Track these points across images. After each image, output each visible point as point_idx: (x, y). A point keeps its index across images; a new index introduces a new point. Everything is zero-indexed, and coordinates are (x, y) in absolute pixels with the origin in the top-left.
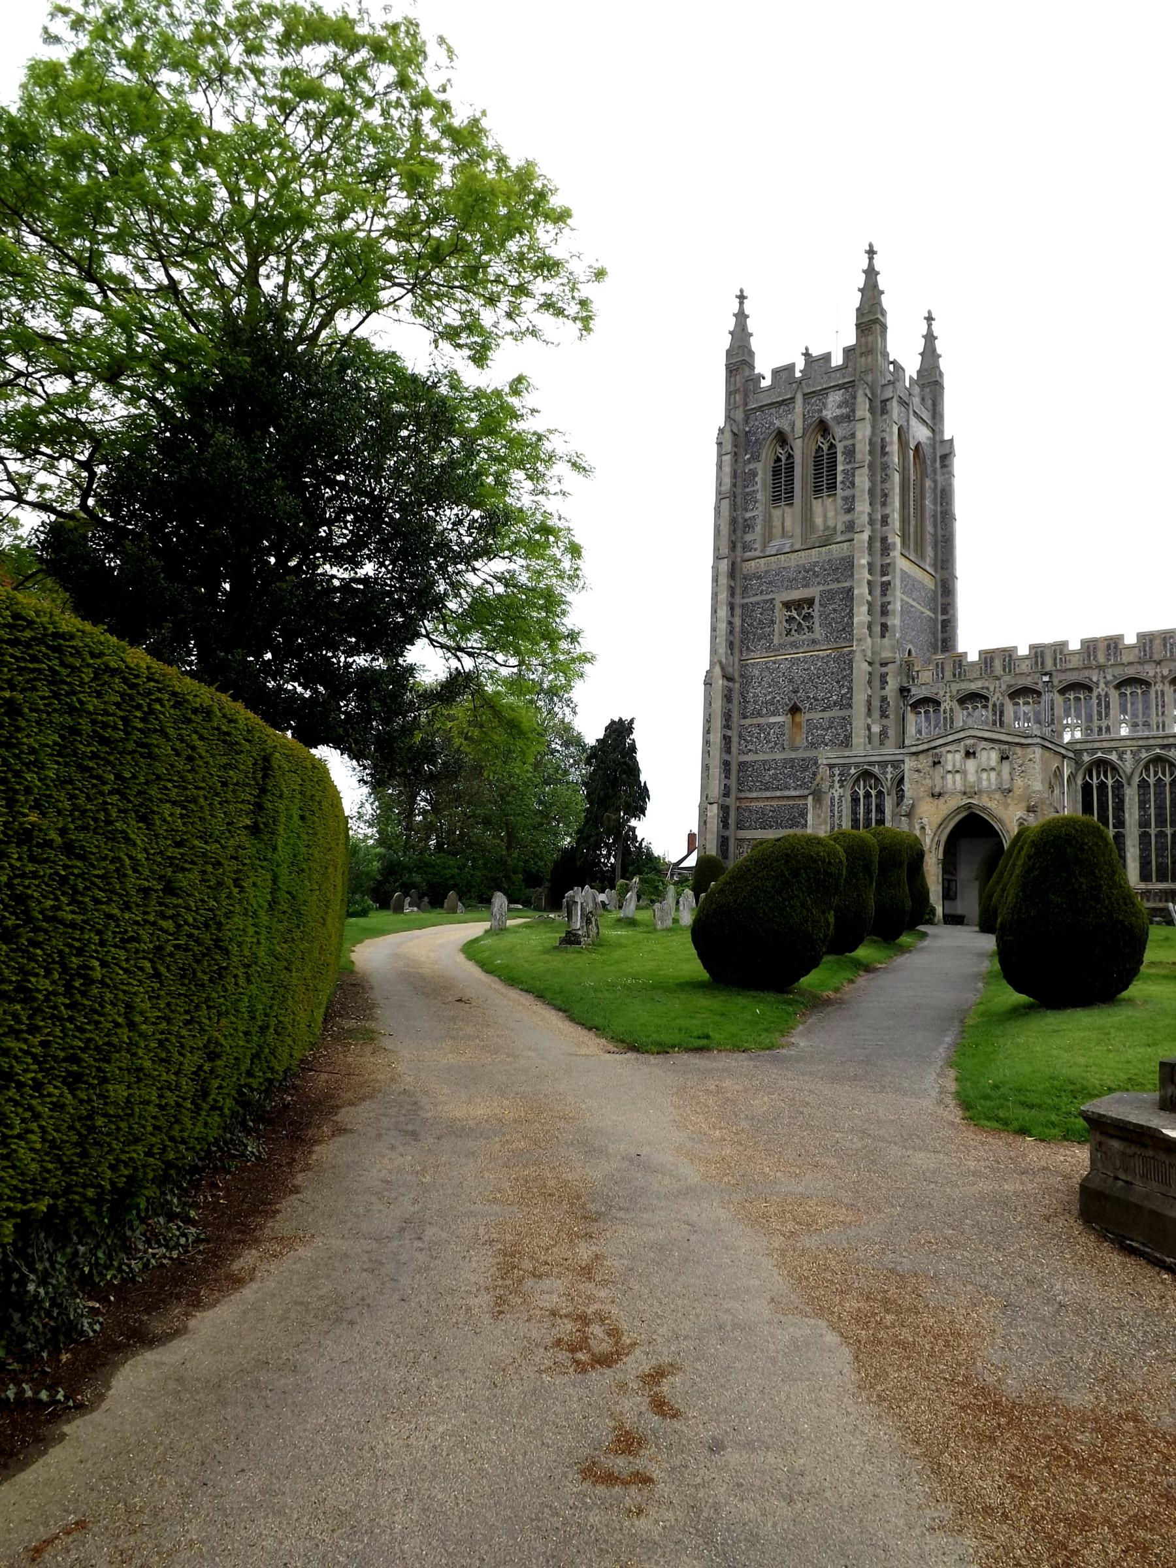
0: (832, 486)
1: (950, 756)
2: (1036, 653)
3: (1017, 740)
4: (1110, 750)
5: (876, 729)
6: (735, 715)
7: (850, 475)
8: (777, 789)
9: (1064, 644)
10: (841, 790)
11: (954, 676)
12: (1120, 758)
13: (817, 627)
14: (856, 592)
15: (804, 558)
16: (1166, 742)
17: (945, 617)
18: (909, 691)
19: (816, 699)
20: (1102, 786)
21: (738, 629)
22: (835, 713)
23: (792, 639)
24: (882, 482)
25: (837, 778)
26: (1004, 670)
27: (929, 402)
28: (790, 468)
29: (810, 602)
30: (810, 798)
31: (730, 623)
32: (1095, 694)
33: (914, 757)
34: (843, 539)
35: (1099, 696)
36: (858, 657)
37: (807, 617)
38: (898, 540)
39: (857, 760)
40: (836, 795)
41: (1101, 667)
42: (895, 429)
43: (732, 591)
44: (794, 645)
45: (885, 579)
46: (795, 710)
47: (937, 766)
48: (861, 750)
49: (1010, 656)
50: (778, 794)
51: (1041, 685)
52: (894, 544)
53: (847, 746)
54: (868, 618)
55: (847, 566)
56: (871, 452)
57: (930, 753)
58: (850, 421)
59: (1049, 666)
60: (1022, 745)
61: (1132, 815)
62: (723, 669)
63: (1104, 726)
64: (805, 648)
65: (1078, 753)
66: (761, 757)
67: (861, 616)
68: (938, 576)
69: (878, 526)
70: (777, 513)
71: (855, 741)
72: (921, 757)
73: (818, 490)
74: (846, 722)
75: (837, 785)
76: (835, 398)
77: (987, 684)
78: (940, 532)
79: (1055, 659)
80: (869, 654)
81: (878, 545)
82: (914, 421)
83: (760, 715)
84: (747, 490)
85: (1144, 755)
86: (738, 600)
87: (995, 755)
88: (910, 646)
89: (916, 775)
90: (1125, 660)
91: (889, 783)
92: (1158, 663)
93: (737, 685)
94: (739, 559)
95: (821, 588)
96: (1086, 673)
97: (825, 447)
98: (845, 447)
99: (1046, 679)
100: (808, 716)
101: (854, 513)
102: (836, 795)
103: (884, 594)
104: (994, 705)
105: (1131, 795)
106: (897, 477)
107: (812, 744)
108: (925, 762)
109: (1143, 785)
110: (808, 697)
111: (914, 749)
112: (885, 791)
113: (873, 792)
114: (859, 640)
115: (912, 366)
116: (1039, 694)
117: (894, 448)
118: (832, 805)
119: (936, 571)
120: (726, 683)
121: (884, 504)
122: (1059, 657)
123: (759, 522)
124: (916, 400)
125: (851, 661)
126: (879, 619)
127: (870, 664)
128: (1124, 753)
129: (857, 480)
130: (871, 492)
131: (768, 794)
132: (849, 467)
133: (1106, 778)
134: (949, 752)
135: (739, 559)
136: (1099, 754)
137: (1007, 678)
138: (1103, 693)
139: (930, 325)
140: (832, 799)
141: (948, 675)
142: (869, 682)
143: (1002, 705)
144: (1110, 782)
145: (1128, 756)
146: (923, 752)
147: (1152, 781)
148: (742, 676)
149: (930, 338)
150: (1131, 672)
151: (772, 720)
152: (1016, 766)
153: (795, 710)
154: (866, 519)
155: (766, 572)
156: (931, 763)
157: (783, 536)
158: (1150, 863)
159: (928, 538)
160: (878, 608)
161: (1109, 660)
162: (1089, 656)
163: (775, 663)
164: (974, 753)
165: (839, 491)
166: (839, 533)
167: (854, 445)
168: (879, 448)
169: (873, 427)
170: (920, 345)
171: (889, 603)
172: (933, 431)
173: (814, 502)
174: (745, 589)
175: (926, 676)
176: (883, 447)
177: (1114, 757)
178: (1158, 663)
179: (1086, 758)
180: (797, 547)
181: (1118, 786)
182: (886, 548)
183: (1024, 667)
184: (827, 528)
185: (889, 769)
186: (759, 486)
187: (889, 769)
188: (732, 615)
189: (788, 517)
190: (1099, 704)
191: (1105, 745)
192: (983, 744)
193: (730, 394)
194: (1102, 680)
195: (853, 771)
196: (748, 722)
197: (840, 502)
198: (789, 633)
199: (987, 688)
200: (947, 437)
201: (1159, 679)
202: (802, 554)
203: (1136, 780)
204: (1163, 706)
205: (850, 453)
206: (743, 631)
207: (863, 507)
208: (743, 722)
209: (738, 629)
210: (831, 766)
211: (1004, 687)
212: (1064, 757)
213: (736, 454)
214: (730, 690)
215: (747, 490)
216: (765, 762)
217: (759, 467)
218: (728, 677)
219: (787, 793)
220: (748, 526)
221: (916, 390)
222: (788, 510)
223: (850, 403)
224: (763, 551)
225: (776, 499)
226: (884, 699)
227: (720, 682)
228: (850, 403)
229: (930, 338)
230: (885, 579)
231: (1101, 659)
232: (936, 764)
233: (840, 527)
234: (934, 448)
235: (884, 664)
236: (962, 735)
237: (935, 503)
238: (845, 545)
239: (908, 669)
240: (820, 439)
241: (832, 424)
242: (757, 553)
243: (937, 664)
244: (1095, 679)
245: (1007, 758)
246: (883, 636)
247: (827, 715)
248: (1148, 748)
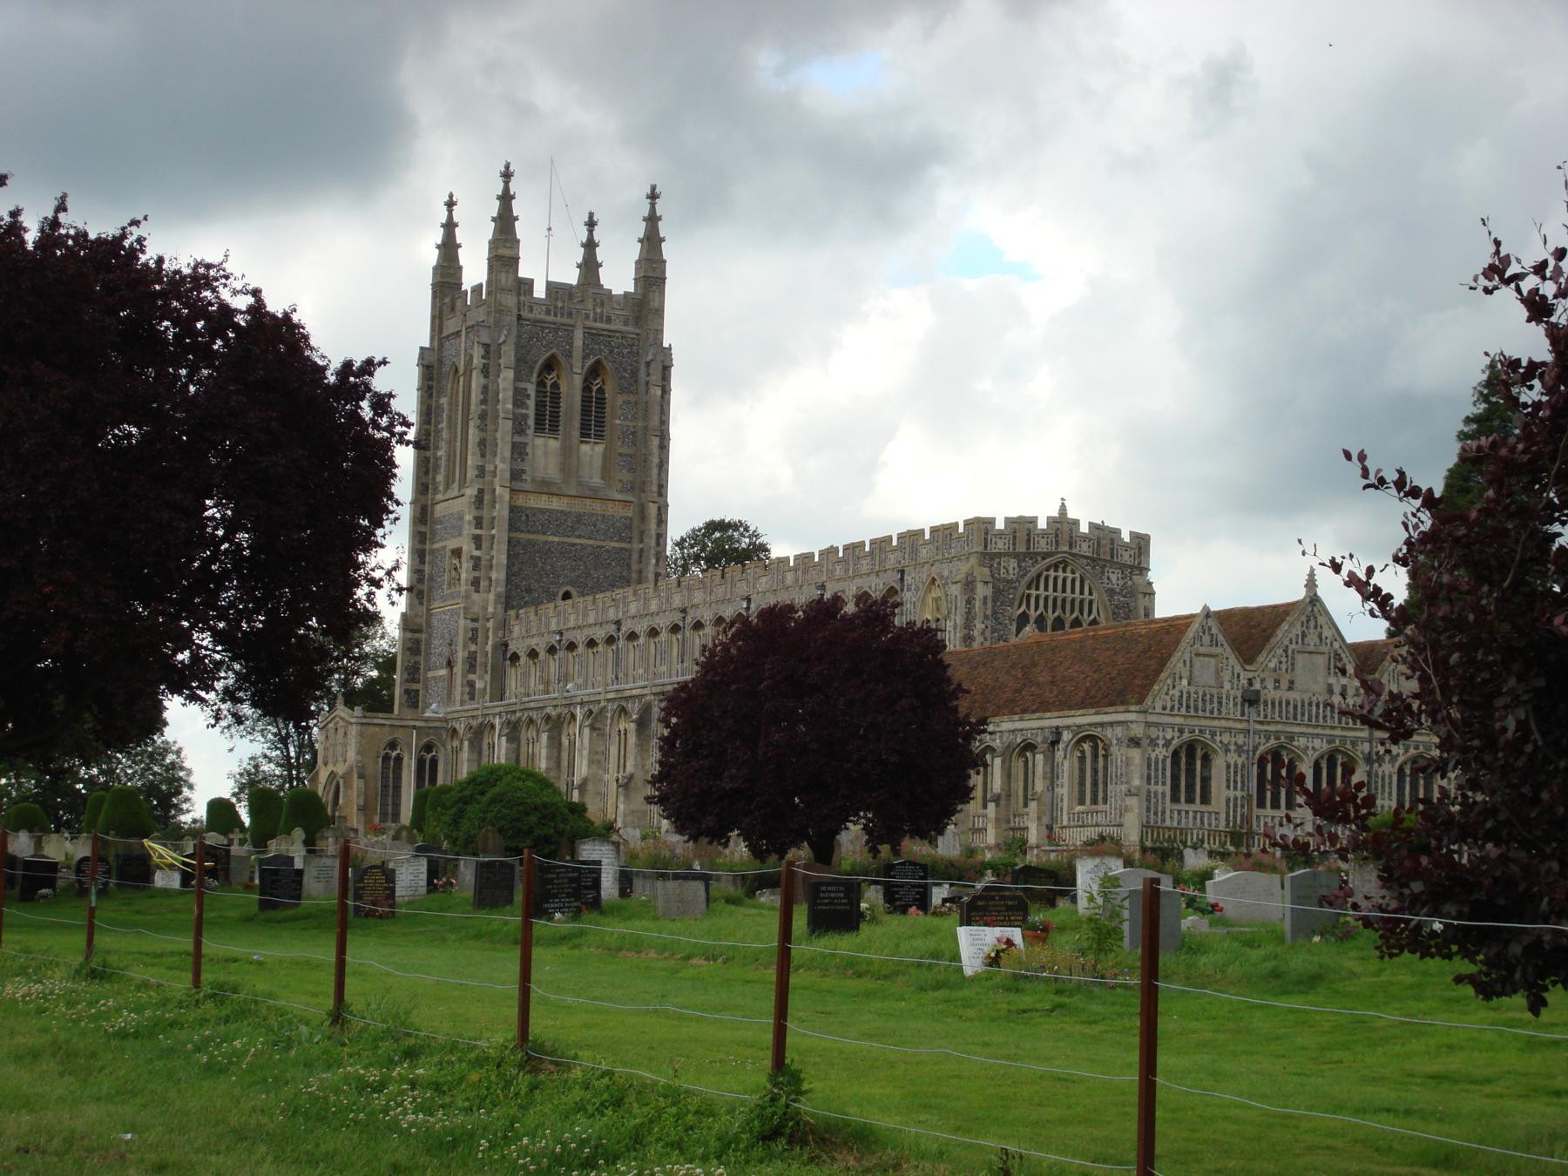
86: (427, 547)
120: (409, 635)
123: (443, 463)
130: (482, 443)
186: (444, 425)
193: (433, 318)
196: (430, 674)
212: (414, 727)
213: (430, 388)
214: (418, 642)
217: (444, 401)
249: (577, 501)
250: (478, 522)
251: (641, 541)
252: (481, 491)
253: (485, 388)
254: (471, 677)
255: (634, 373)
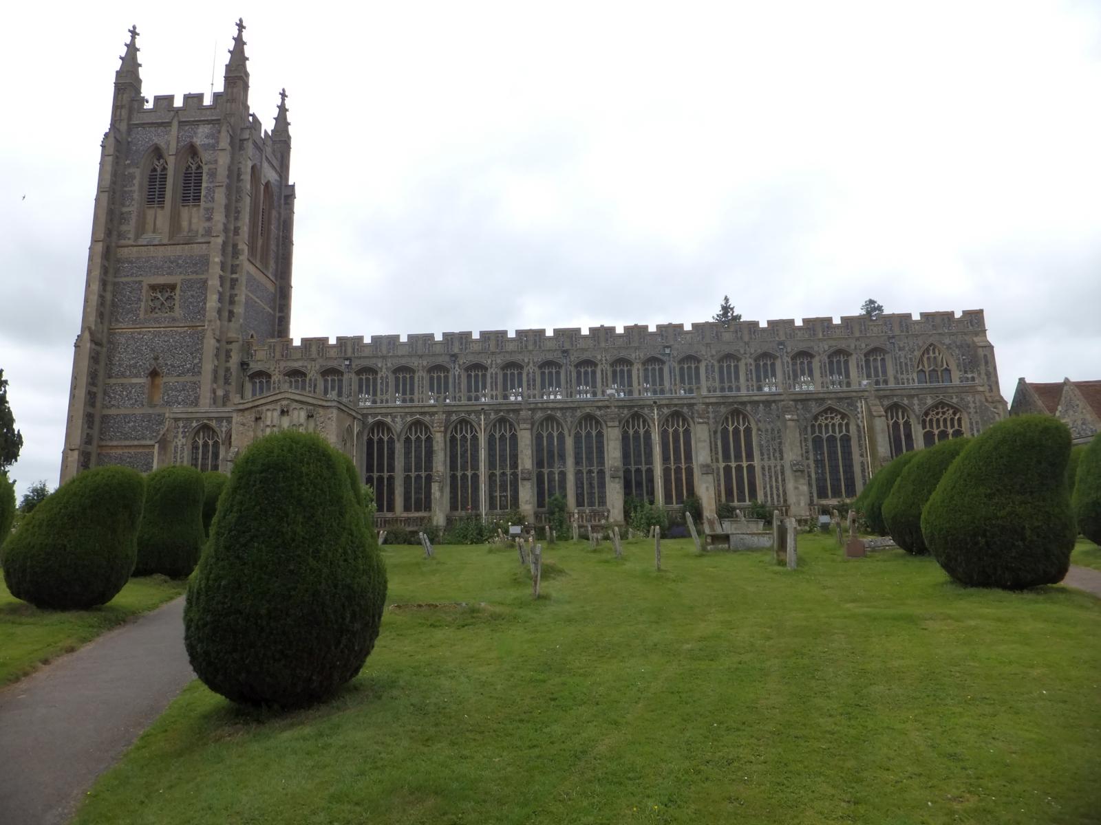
0: (197, 199)
1: (269, 414)
2: (341, 343)
3: (320, 403)
4: (386, 415)
5: (220, 393)
6: (101, 374)
7: (211, 191)
8: (135, 439)
9: (361, 338)
10: (184, 440)
11: (283, 356)
12: (393, 421)
13: (177, 307)
14: (210, 283)
15: (171, 252)
16: (423, 410)
17: (281, 314)
18: (248, 365)
19: (173, 366)
20: (381, 441)
21: (108, 303)
22: (188, 378)
23: (156, 315)
24: (236, 202)
25: (181, 430)
26: (319, 354)
27: (279, 155)
28: (164, 178)
29: (173, 287)
30: (157, 445)
31: (101, 297)
32: (379, 376)
33: (240, 414)
34: (203, 240)
35: (382, 378)
36: (209, 334)
37: (170, 298)
38: (246, 248)
39: (198, 415)
40: (179, 444)
41: (384, 357)
42: (250, 164)
43: (105, 270)
44: (156, 320)
45: (234, 276)
46: (154, 374)
47: (259, 421)
48: (205, 407)
49: (323, 344)
50: (136, 443)
51: (343, 367)
52: (243, 250)
53: (196, 405)
54: (219, 305)
55: (204, 262)
56: (229, 177)
57: (253, 410)
58: (214, 150)
59: (349, 354)
60: (323, 407)
61: (399, 463)
62: (91, 333)
63: (384, 398)
64: (166, 324)
65: (365, 416)
66: (123, 411)
67: (212, 302)
68: (278, 283)
69: (231, 234)
70: (150, 213)
71: (202, 401)
72: (246, 413)
73: (185, 200)
74: (196, 386)
75: (180, 436)
76: (204, 130)
77: (306, 364)
78: (281, 251)
79: (354, 349)
80: (218, 333)
81: (230, 249)
82: (265, 165)
83: (123, 376)
84: (126, 189)
85: (409, 419)
87: (303, 414)
88: (253, 332)
89: (241, 428)
90: (400, 353)
91: (224, 436)
92: (421, 357)
93: (105, 349)
94: (113, 244)
95: (182, 277)
96: (374, 361)
97: (194, 167)
98: (209, 169)
99: (347, 363)
100: (165, 379)
101: (207, 218)
102: (179, 444)
103: (232, 287)
104: (310, 380)
105: (399, 447)
106: (248, 200)
107: (168, 403)
108: (249, 417)
109: (408, 440)
110: (166, 364)
111: (241, 407)
112: (220, 441)
113: (210, 442)
114: (210, 321)
115: (268, 125)
116: (342, 373)
117: (247, 177)
118: (176, 452)
119: (276, 280)
120: (94, 346)
121: (237, 219)
122: (356, 347)
124: (269, 150)
125: (203, 338)
126: (227, 307)
127: (218, 341)
128: (396, 417)
129: (216, 195)
130: (227, 207)
131: (127, 443)
132: (211, 185)
133: (383, 435)
134: (268, 410)
135: (113, 244)
136: (379, 417)
137: (320, 361)
138: (384, 376)
139: (283, 100)
140: (176, 447)
141: (278, 355)
142: (217, 355)
143: (316, 380)
144: (386, 439)
145: (398, 420)
146: (247, 409)
147: (413, 438)
148: (110, 342)
149: (283, 109)
150: (403, 362)
151: (135, 381)
152: (318, 423)
153: (154, 374)
154: (220, 227)
155: (138, 258)
156: (253, 419)
157: (154, 231)
158: (411, 498)
159: (272, 255)
160: (227, 298)
161: (389, 352)
162: (377, 348)
163: (139, 333)
164: (288, 412)
165: (202, 203)
166: (200, 236)
167: (216, 169)
168: (234, 174)
169: (232, 158)
170: (275, 112)
171: (236, 295)
172: (280, 176)
173: (182, 208)
174: (117, 271)
175: (261, 355)
176: (239, 175)
177: (388, 420)
178: (421, 357)
179: (371, 420)
180: (165, 241)
181: (391, 441)
182: (236, 253)
183: (333, 353)
184: (190, 230)
185: (224, 424)
187: (224, 424)
188: (104, 290)
189: (160, 218)
190: (382, 383)
191: (384, 411)
192: (295, 405)
194: (384, 367)
195: (194, 424)
196: (113, 381)
197: (202, 211)
198: (153, 310)
199: (306, 367)
200: (291, 183)
201: (421, 368)
202: (169, 248)
203: (403, 437)
204: (422, 387)
205: (213, 174)
206: (113, 304)
207: (219, 217)
208: (108, 381)
209: (108, 303)
210: (176, 420)
211: (318, 367)
212: (355, 418)
214: (98, 353)
215: (126, 189)
216: (125, 416)
218: (94, 341)
219: (143, 442)
220: (123, 218)
221: (269, 142)
222: (159, 212)
223: (215, 136)
224: (135, 240)
225: (150, 201)
226: (228, 370)
227: (88, 345)
228: (215, 136)
229: (283, 109)
230: (234, 276)
231: (385, 352)
232: (258, 419)
233: (201, 231)
234: (280, 189)
235: (229, 343)
236: (279, 397)
237: (278, 229)
238: (204, 246)
239: (247, 348)
240: (190, 159)
241: (200, 149)
242: (131, 242)
243: (270, 347)
244: (380, 365)
245: (312, 416)
246: (230, 321)
247: (181, 379)
248: (412, 414)
249: (258, 272)
250: (223, 266)
251: (281, 310)
252: (225, 244)
253: (230, 169)
254: (215, 386)
255: (280, 199)
